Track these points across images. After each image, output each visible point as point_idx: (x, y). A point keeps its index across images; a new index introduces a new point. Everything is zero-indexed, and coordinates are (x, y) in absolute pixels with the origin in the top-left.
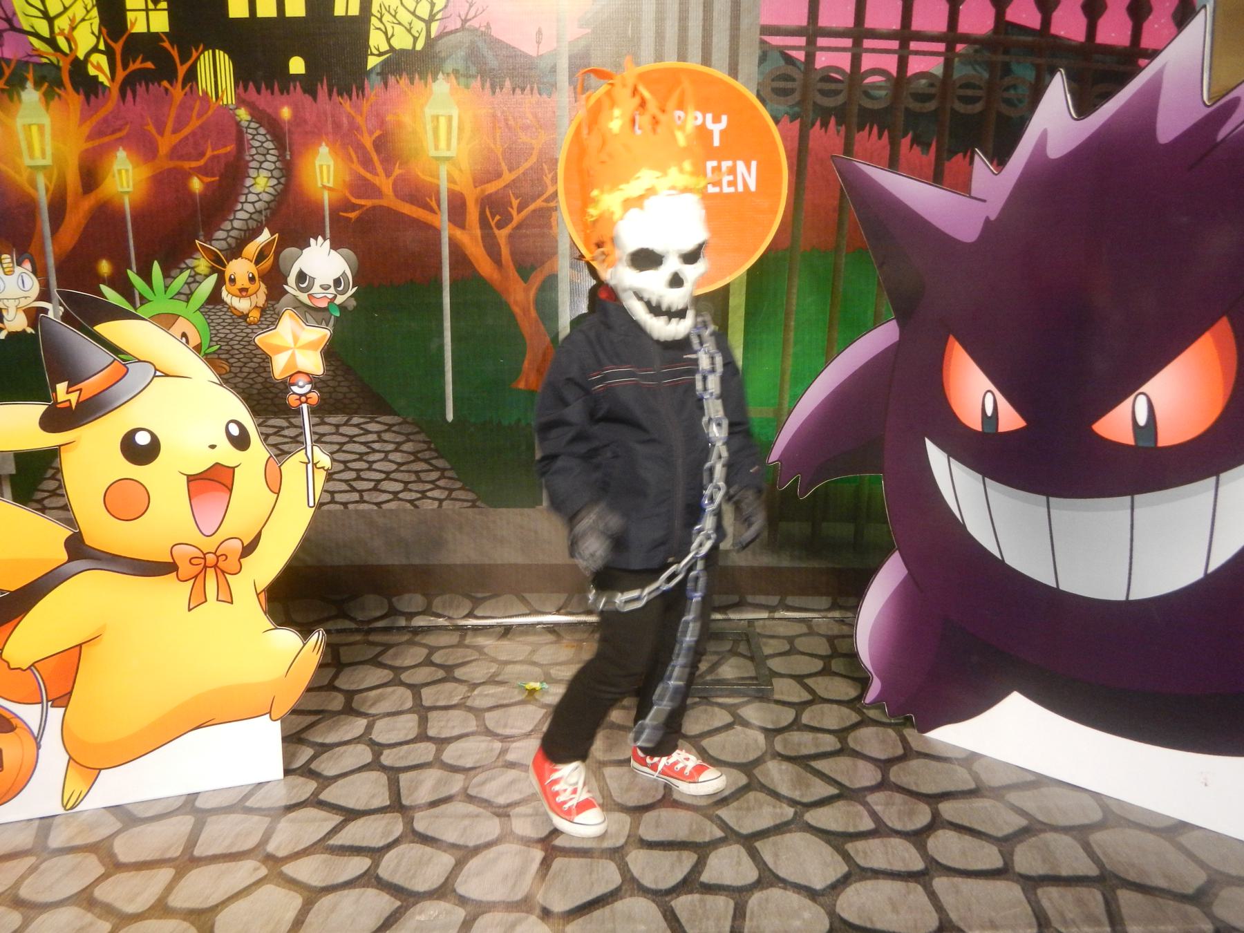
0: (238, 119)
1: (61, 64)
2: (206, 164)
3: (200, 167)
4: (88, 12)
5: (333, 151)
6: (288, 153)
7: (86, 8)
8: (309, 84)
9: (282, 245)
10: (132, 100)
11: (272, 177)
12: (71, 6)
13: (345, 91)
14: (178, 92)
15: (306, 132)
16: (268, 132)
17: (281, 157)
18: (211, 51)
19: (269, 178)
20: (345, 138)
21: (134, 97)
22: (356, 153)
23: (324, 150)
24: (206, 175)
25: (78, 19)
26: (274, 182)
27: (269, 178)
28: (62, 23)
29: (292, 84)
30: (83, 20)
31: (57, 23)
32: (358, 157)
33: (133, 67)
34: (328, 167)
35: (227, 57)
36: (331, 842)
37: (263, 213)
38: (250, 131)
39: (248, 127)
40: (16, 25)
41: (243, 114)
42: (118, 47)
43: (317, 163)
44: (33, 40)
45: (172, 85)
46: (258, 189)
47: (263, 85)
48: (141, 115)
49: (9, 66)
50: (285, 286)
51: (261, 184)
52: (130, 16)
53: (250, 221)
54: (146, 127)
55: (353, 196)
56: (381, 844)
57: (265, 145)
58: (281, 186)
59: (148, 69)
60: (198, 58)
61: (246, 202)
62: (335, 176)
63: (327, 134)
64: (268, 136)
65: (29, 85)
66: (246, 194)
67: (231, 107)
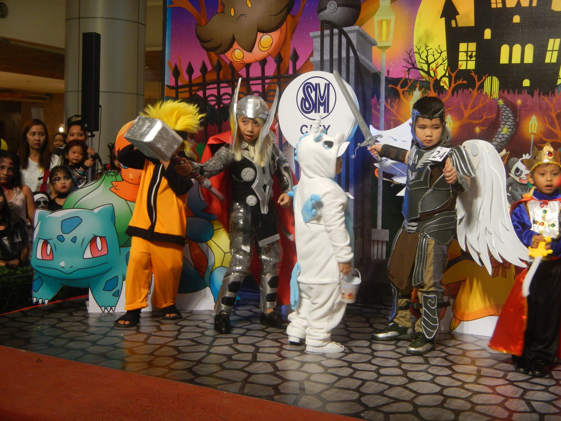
0: (499, 104)
1: (430, 81)
2: (483, 122)
3: (480, 123)
4: (444, 61)
5: (538, 118)
6: (518, 118)
7: (443, 60)
8: (530, 91)
9: (511, 156)
10: (456, 96)
11: (510, 128)
12: (437, 59)
13: (546, 94)
14: (475, 93)
15: (527, 110)
16: (511, 110)
17: (515, 120)
18: (491, 77)
19: (508, 128)
20: (543, 113)
21: (457, 94)
22: (548, 119)
23: (534, 118)
24: (482, 126)
25: (439, 65)
26: (510, 130)
27: (508, 128)
28: (433, 66)
29: (523, 91)
30: (441, 64)
31: (431, 65)
32: (548, 121)
33: (458, 83)
34: (535, 125)
35: (497, 79)
36: (529, 381)
37: (504, 143)
38: (503, 109)
39: (502, 107)
40: (415, 66)
41: (501, 102)
42: (453, 75)
43: (530, 123)
44: (421, 72)
45: (473, 89)
46: (503, 133)
47: (511, 90)
48: (459, 102)
49: (410, 82)
50: (510, 174)
51: (505, 130)
52: (460, 63)
53: (498, 146)
54: (460, 106)
55: (545, 137)
56: (548, 385)
57: (508, 115)
58: (513, 132)
59: (465, 84)
60: (485, 79)
61: (497, 138)
62: (537, 131)
63: (536, 111)
64: (510, 111)
65: (417, 89)
66: (498, 135)
67: (497, 99)
